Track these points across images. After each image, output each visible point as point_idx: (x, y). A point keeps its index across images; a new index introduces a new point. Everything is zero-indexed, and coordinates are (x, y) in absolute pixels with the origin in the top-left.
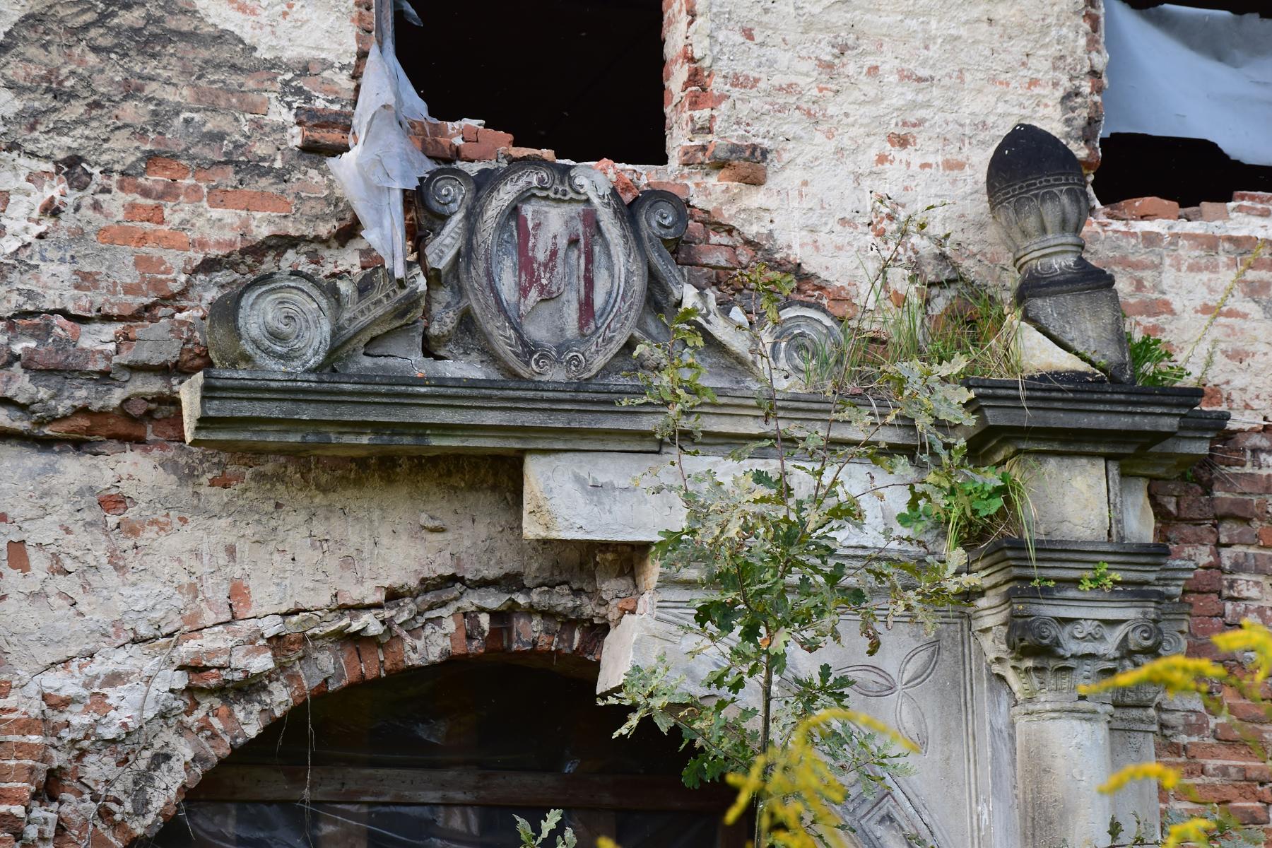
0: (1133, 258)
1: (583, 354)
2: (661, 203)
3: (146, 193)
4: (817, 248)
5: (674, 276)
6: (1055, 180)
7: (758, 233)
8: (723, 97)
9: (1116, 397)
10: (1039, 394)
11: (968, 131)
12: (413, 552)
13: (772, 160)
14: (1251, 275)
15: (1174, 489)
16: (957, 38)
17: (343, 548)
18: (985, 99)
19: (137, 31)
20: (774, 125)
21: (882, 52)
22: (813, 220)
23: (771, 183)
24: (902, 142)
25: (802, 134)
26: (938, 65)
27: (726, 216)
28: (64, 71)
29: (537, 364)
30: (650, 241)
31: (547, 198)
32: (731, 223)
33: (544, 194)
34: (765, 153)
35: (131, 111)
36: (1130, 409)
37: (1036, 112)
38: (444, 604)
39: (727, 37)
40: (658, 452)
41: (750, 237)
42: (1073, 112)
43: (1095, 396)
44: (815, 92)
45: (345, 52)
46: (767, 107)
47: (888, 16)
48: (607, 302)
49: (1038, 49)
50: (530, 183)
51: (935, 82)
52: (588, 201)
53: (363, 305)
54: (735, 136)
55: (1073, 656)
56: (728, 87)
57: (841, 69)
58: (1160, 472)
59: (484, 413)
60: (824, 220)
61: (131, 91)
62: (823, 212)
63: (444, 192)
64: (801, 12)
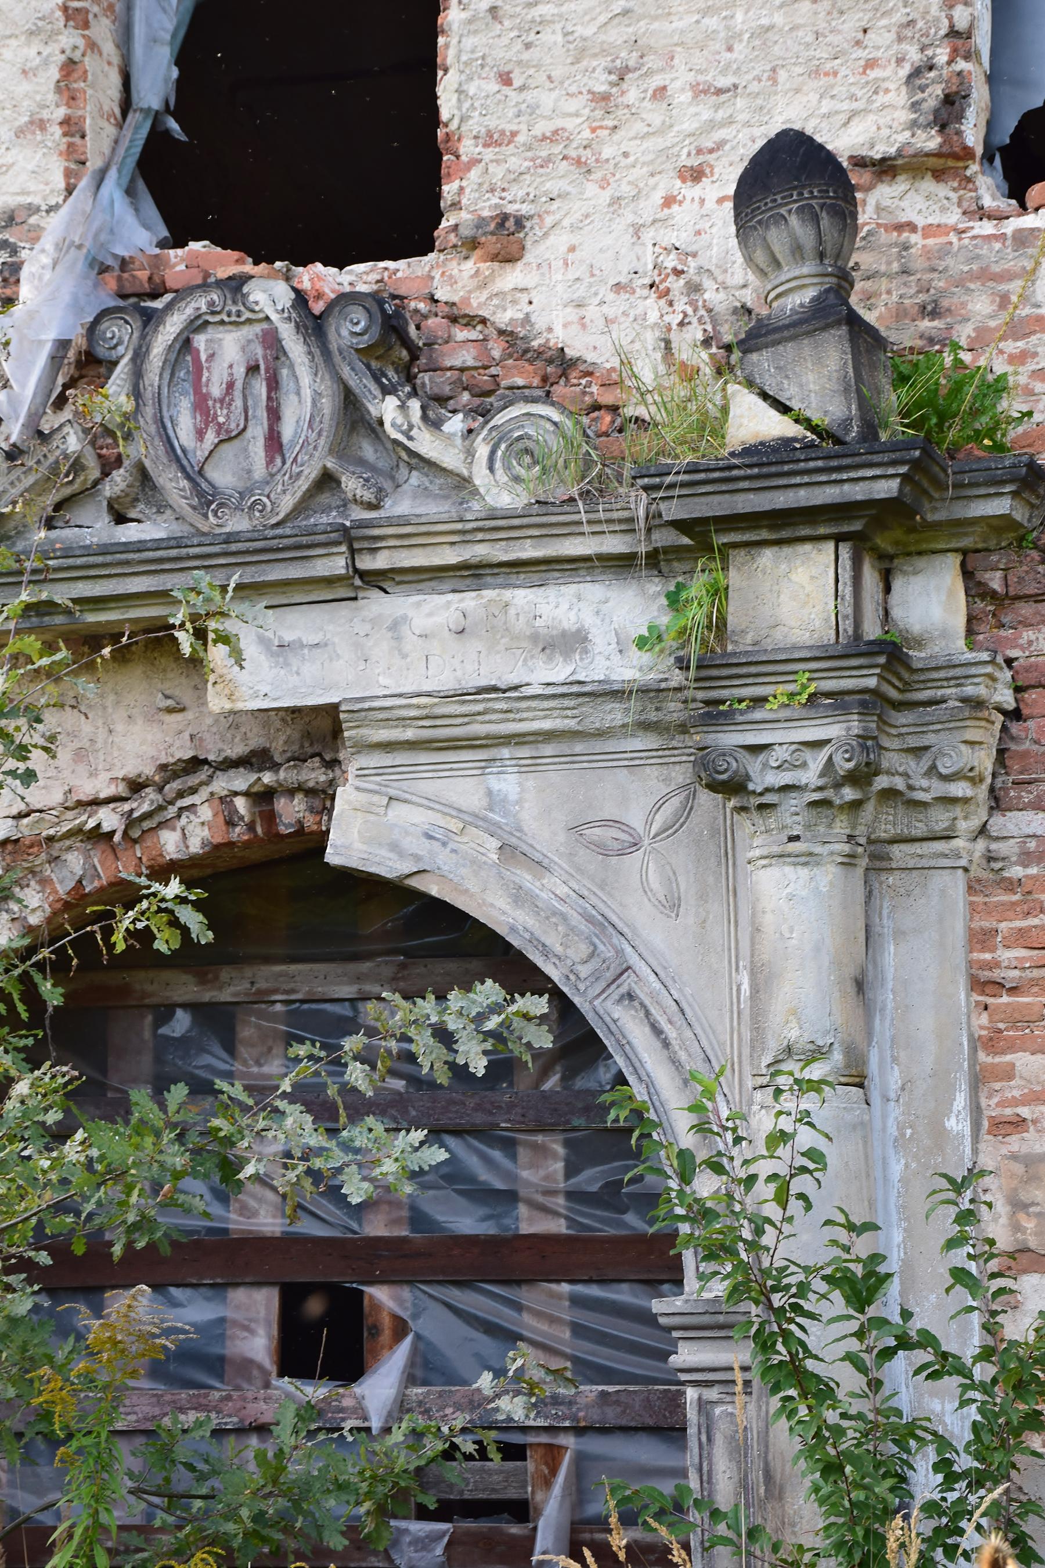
0: (996, 269)
1: (268, 497)
2: (351, 307)
4: (584, 326)
5: (370, 391)
6: (783, 198)
7: (511, 319)
9: (812, 464)
10: (716, 475)
12: (150, 737)
13: (532, 228)
15: (998, 561)
16: (769, 28)
17: (76, 740)
18: (805, 99)
20: (535, 185)
21: (673, 67)
22: (581, 291)
23: (529, 257)
25: (569, 189)
26: (744, 69)
27: (475, 305)
29: (215, 515)
30: (341, 354)
31: (222, 322)
32: (480, 313)
33: (217, 318)
34: (520, 222)
36: (834, 476)
37: (873, 102)
38: (193, 791)
39: (479, 88)
40: (355, 599)
41: (503, 327)
42: (923, 92)
43: (786, 468)
44: (587, 134)
45: (52, 191)
46: (527, 164)
47: (681, 19)
48: (296, 432)
49: (879, 19)
50: (198, 309)
51: (739, 90)
52: (267, 318)
53: (13, 476)
55: (767, 790)
56: (480, 149)
57: (620, 99)
58: (966, 542)
59: (128, 580)
60: (593, 290)
62: (592, 280)
63: (109, 335)
64: (571, 38)
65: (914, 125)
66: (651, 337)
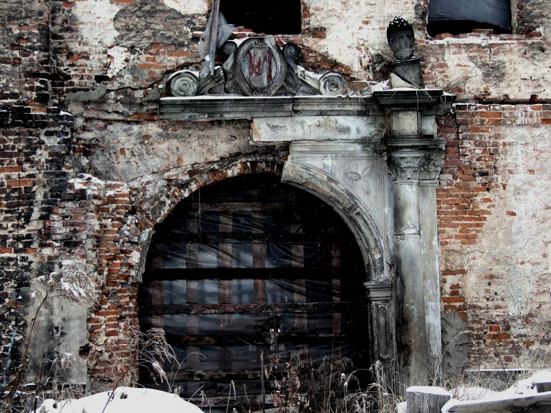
3: (151, 54)
8: (313, 14)
11: (386, 18)
14: (471, 54)
19: (148, 11)
24: (367, 23)
28: (130, 23)
34: (325, 29)
35: (147, 33)
54: (316, 25)
61: (147, 27)
65: (416, 18)
66: (357, 59)
